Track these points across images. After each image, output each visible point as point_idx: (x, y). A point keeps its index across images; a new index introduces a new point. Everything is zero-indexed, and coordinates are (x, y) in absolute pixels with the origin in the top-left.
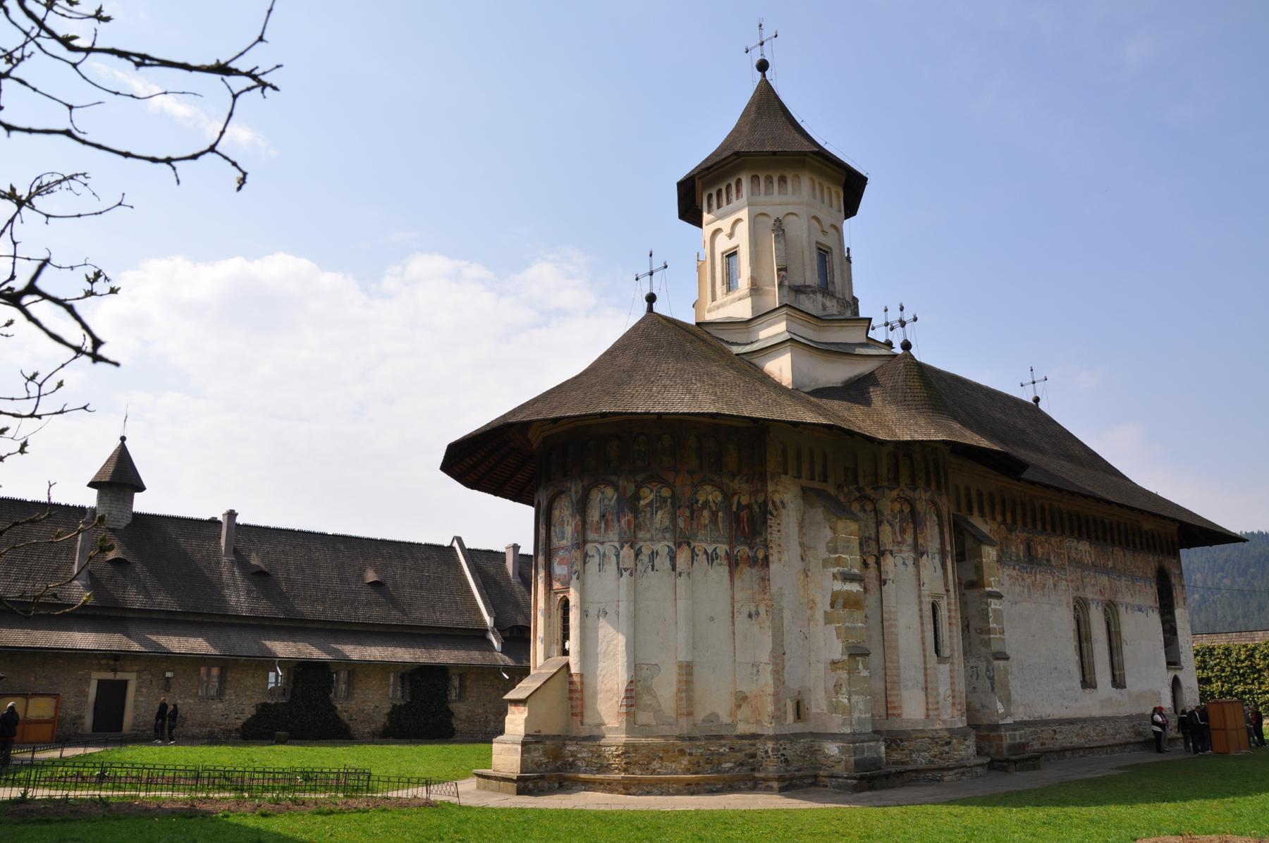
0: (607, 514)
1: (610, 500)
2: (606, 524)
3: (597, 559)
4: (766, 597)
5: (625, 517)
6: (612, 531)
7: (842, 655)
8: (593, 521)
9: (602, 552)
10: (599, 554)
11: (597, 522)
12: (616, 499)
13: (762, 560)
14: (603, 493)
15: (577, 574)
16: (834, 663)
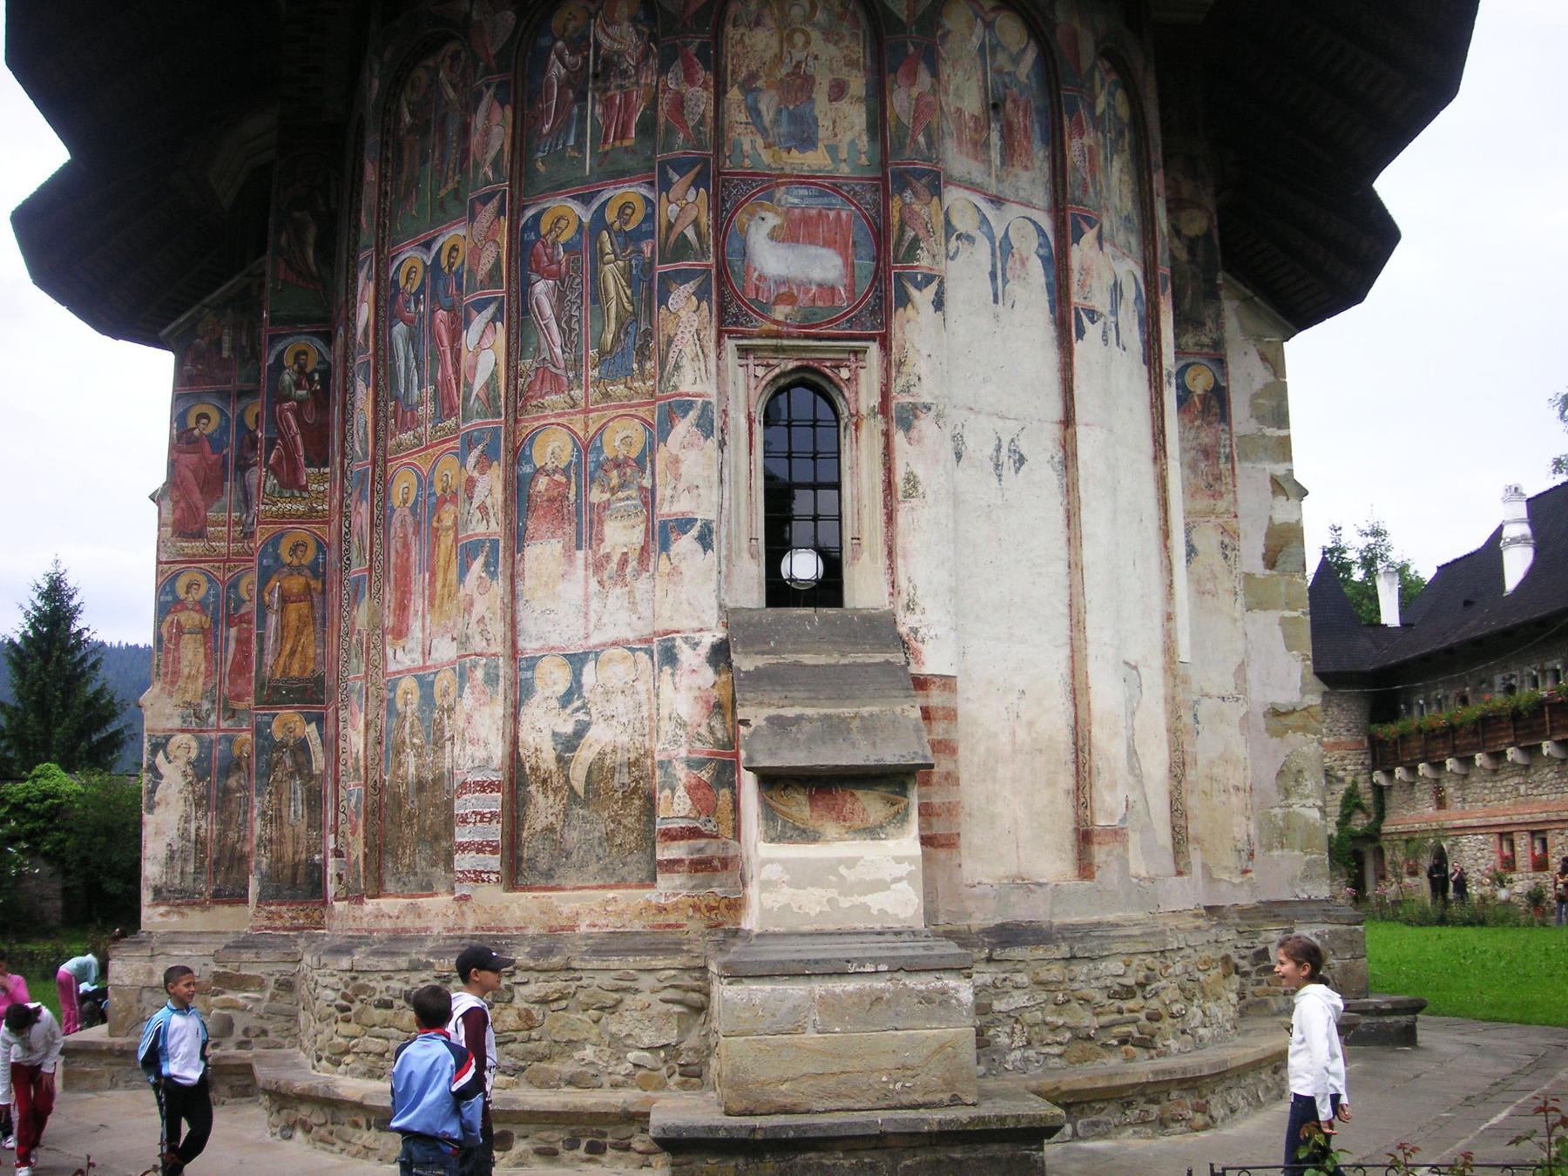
0: (1009, 105)
1: (1016, 60)
2: (1007, 134)
3: (982, 250)
4: (1222, 505)
5: (1081, 135)
6: (1026, 168)
7: (1303, 692)
8: (959, 111)
9: (999, 233)
10: (991, 239)
11: (975, 118)
12: (1036, 62)
13: (1204, 398)
14: (989, 25)
15: (933, 287)
16: (1275, 713)
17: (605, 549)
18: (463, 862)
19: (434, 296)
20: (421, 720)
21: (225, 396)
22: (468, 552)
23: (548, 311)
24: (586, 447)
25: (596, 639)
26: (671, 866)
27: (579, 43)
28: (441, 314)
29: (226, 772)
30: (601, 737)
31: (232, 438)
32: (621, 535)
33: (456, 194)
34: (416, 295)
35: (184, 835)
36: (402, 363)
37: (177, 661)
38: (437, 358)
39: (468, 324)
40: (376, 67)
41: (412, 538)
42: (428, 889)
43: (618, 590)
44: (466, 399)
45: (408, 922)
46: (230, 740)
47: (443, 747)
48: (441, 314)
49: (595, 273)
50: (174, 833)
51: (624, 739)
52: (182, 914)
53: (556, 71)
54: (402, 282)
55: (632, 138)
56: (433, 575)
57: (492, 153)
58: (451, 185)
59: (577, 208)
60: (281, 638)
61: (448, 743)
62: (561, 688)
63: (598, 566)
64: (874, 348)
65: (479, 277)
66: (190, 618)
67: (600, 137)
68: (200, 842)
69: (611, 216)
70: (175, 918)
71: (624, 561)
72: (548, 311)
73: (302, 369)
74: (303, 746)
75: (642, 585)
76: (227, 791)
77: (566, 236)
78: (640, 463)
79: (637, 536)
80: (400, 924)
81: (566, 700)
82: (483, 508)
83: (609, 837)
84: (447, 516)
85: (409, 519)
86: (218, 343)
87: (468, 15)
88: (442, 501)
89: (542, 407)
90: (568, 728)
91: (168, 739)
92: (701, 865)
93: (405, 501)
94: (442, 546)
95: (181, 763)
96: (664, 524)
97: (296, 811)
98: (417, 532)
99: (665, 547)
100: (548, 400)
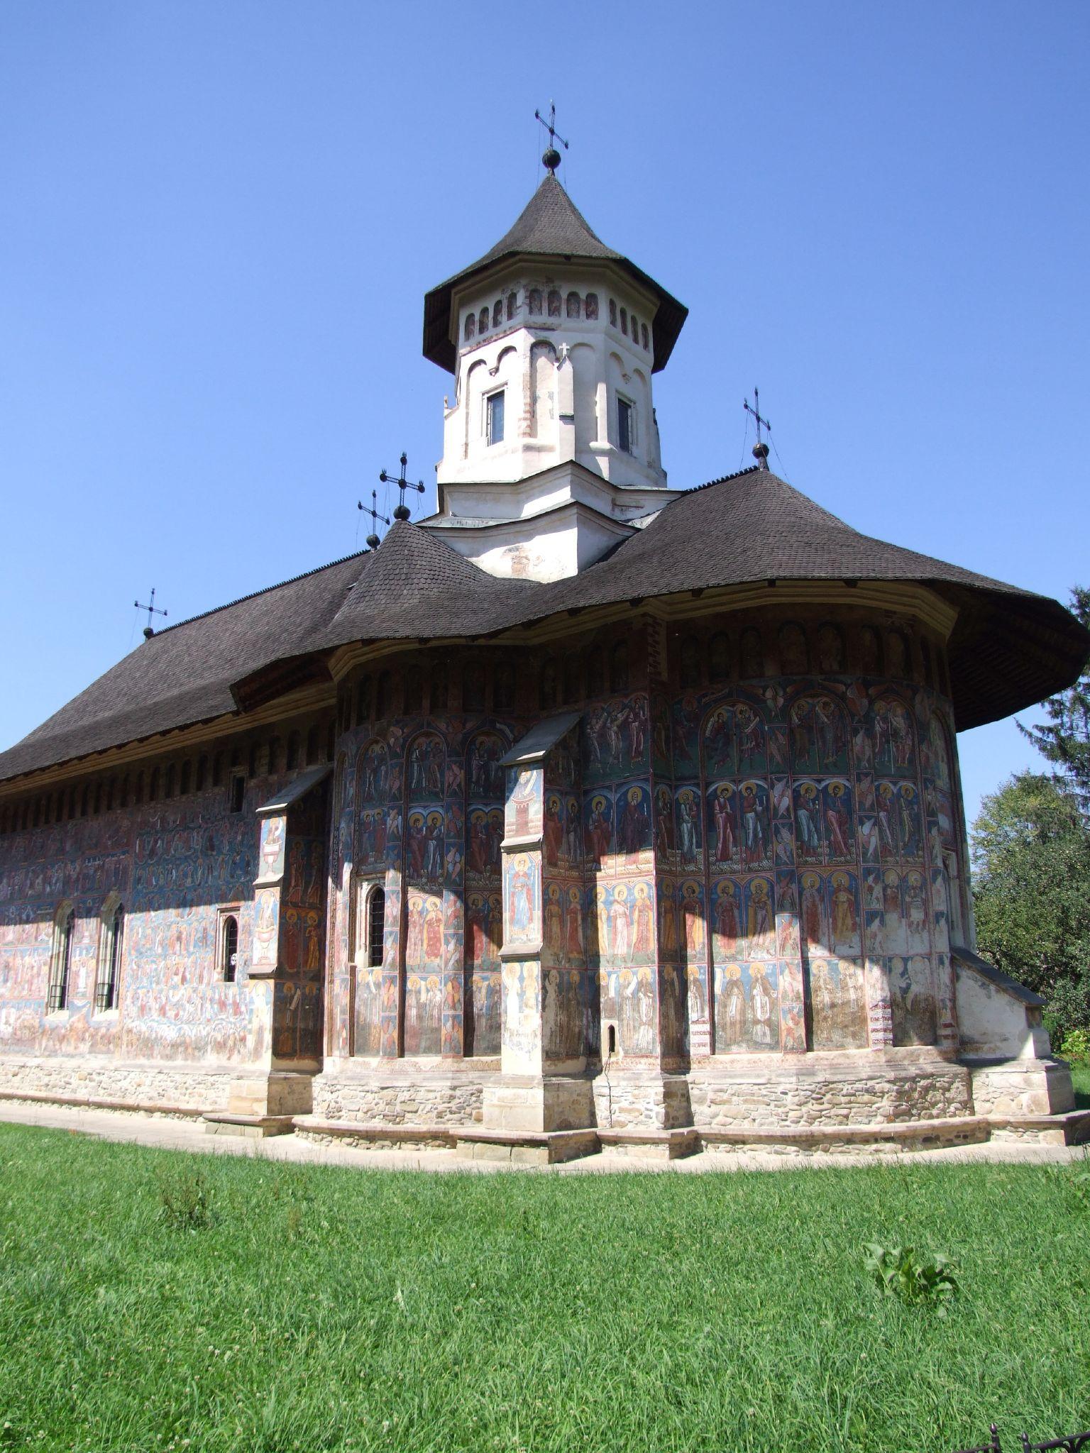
17: (912, 919)
18: (873, 1036)
19: (825, 803)
20: (832, 979)
21: (562, 793)
22: (872, 916)
23: (885, 824)
24: (904, 879)
25: (912, 952)
26: (946, 1037)
27: (885, 720)
28: (831, 813)
29: (568, 990)
30: (915, 988)
31: (564, 817)
32: (917, 915)
33: (835, 765)
34: (814, 801)
35: (556, 1026)
36: (806, 827)
37: (551, 931)
38: (829, 830)
39: (862, 823)
40: (781, 693)
41: (817, 902)
42: (842, 1047)
43: (917, 935)
44: (865, 854)
45: (841, 1060)
46: (569, 973)
47: (848, 990)
48: (831, 813)
49: (900, 814)
50: (553, 1023)
51: (922, 990)
52: (556, 1065)
53: (878, 728)
54: (802, 792)
55: (906, 765)
56: (835, 919)
57: (866, 757)
58: (831, 759)
59: (892, 787)
60: (665, 930)
61: (852, 991)
62: (901, 970)
63: (910, 925)
64: (954, 854)
65: (867, 806)
66: (555, 909)
67: (896, 761)
68: (561, 1027)
69: (903, 792)
70: (553, 1067)
71: (918, 925)
72: (885, 824)
73: (664, 802)
74: (672, 984)
75: (925, 935)
76: (569, 1000)
77: (889, 796)
78: (921, 888)
79: (922, 916)
80: (835, 1062)
81: (903, 974)
82: (877, 899)
83: (920, 1027)
84: (843, 897)
85: (816, 894)
86: (557, 764)
87: (844, 693)
88: (838, 890)
89: (887, 861)
90: (904, 985)
91: (549, 972)
92: (953, 1037)
93: (812, 887)
94: (841, 909)
95: (554, 984)
96: (937, 914)
97: (672, 1013)
98: (822, 900)
99: (938, 922)
100: (889, 859)
